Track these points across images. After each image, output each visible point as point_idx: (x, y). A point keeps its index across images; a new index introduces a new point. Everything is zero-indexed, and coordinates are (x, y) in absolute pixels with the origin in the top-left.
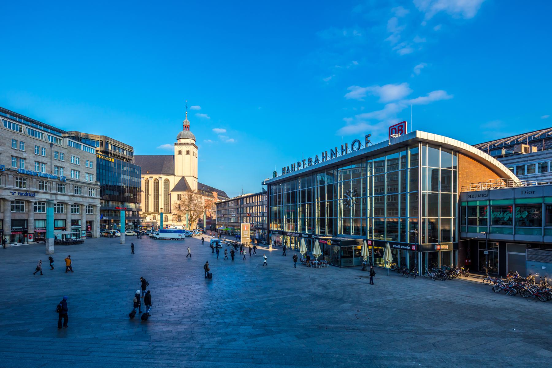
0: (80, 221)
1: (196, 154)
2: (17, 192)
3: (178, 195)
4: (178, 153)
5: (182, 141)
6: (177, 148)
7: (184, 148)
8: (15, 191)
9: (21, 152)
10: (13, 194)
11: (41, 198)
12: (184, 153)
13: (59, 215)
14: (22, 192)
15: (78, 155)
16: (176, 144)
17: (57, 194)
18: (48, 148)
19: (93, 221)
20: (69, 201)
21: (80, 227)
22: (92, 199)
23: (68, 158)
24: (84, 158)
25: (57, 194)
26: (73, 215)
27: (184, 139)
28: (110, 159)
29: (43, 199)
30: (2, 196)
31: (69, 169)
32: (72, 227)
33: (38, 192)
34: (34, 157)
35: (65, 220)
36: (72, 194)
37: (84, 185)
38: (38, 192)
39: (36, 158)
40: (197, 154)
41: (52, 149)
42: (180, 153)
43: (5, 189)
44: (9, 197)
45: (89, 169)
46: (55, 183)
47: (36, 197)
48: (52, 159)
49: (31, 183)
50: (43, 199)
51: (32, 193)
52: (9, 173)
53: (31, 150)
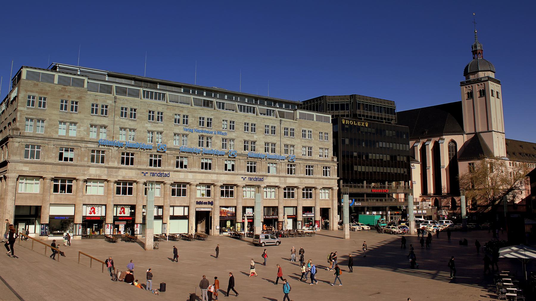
0: (313, 208)
1: (497, 93)
2: (247, 177)
3: (470, 164)
4: (466, 96)
5: (472, 77)
6: (465, 90)
7: (477, 88)
8: (246, 176)
9: (252, 135)
10: (244, 180)
11: (270, 183)
12: (477, 94)
13: (289, 200)
14: (251, 177)
15: (309, 128)
16: (462, 84)
17: (286, 177)
18: (277, 126)
19: (330, 208)
20: (299, 185)
21: (313, 215)
22: (327, 180)
23: (299, 133)
24: (316, 130)
25: (286, 177)
26: (305, 201)
27: (483, 72)
28: (363, 123)
29: (272, 183)
30: (235, 182)
31: (300, 146)
32: (304, 215)
33: (267, 176)
34: (264, 137)
35: (296, 207)
36: (302, 175)
37: (317, 163)
38: (267, 176)
39: (266, 139)
40: (500, 92)
41: (282, 126)
42: (470, 95)
43: (237, 174)
44: (241, 182)
45: (323, 142)
46: (284, 164)
47: (265, 181)
48: (282, 137)
49: (260, 167)
50: (272, 183)
51: (261, 177)
52: (241, 157)
53: (261, 131)
